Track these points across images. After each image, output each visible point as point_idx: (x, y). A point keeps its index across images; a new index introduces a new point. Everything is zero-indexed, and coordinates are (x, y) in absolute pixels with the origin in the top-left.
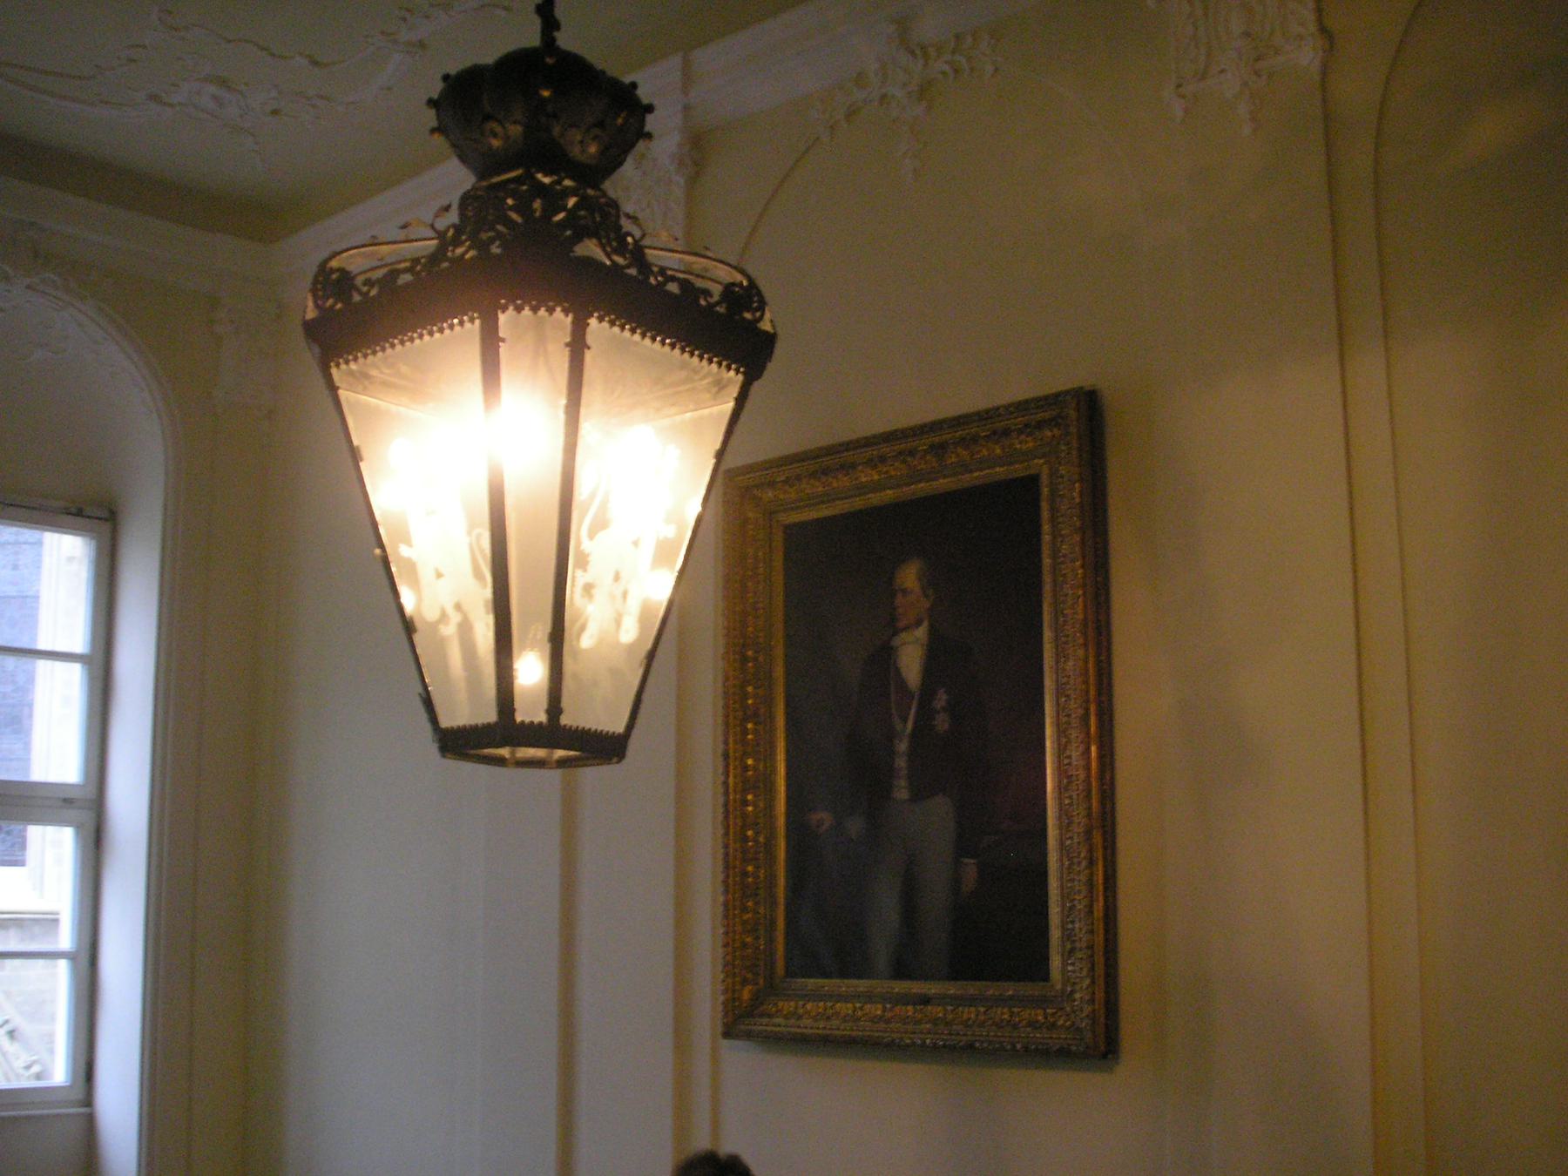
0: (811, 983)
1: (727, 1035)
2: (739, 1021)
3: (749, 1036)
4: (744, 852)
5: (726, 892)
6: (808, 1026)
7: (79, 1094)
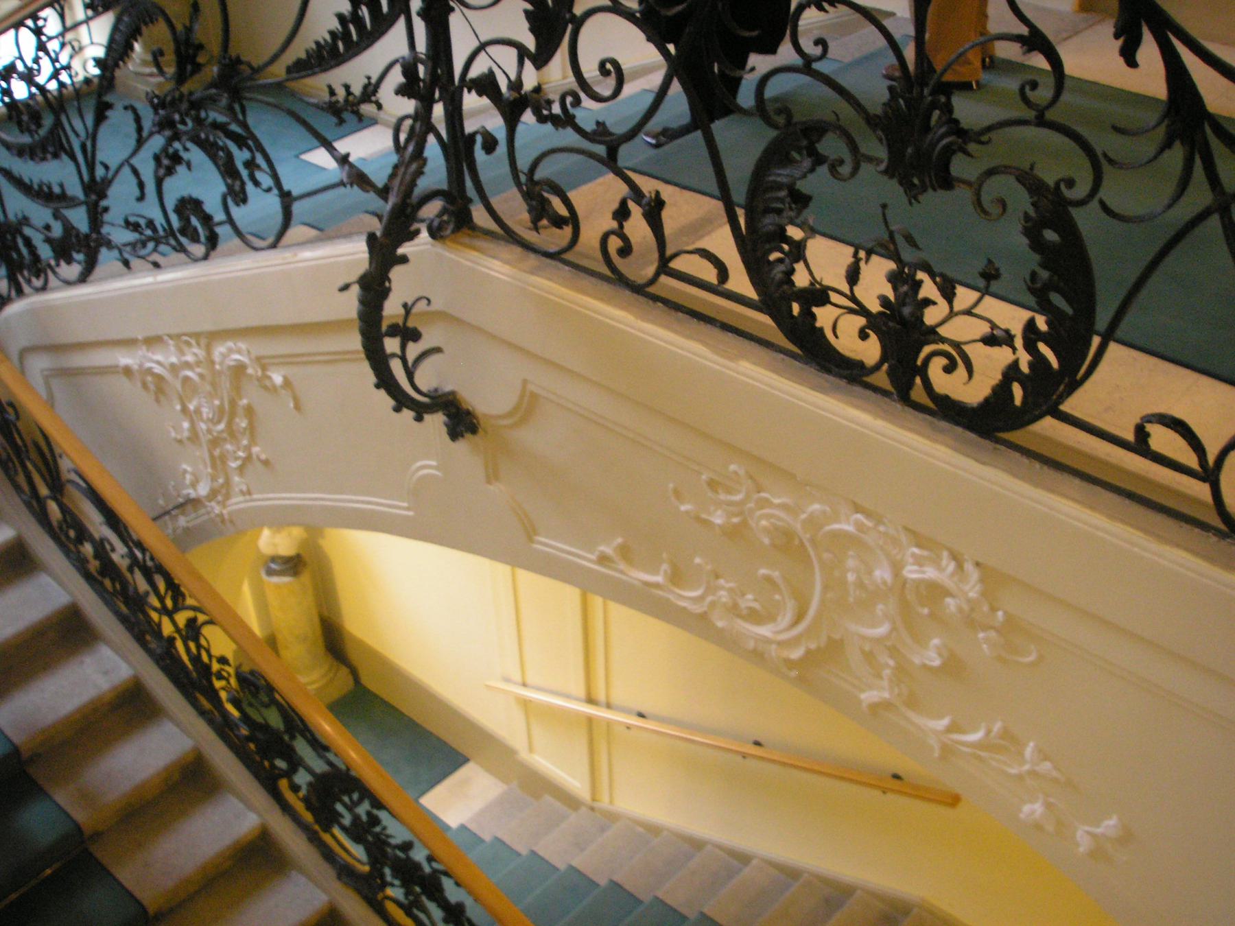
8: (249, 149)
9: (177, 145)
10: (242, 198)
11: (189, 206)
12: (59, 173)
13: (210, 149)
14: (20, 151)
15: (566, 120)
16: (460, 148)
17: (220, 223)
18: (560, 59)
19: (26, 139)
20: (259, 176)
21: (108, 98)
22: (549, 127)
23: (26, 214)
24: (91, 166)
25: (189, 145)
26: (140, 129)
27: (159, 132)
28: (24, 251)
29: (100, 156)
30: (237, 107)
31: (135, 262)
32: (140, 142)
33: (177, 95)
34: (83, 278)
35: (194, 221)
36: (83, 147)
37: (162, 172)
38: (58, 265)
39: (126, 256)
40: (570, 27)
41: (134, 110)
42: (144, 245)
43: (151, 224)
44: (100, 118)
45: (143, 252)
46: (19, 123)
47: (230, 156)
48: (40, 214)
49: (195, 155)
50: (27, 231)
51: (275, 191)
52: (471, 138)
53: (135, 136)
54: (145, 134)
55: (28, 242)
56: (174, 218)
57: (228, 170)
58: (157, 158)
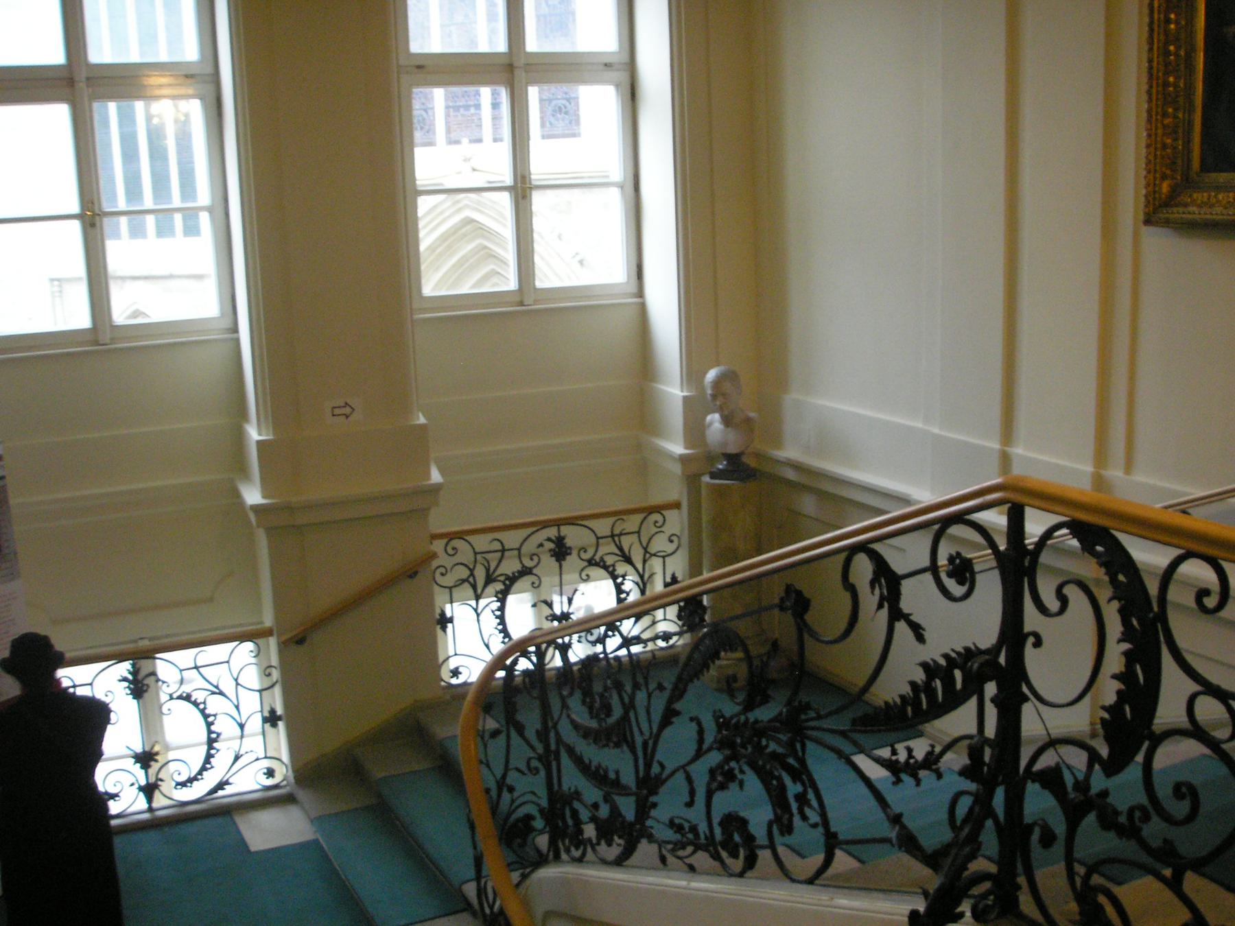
0: (1223, 177)
1: (1148, 222)
2: (1159, 211)
3: (1167, 223)
4: (1167, 64)
5: (1150, 100)
6: (1218, 214)
7: (633, 288)
8: (803, 784)
9: (733, 764)
10: (788, 829)
11: (734, 822)
12: (619, 762)
13: (765, 777)
14: (586, 733)
15: (1130, 831)
16: (1016, 835)
17: (762, 847)
18: (1133, 772)
19: (594, 724)
20: (808, 811)
21: (678, 706)
22: (1111, 835)
23: (580, 789)
24: (648, 766)
25: (746, 768)
26: (701, 741)
27: (719, 749)
28: (570, 822)
29: (658, 757)
30: (798, 746)
31: (670, 859)
32: (699, 754)
33: (743, 718)
34: (619, 862)
35: (737, 838)
36: (645, 744)
37: (714, 785)
38: (598, 844)
39: (664, 852)
40: (1146, 744)
41: (699, 724)
42: (684, 848)
43: (694, 829)
44: (666, 721)
45: (681, 853)
46: (591, 708)
47: (782, 788)
48: (591, 793)
49: (752, 782)
50: (576, 805)
51: (821, 829)
52: (1030, 828)
53: (694, 746)
54: (705, 747)
55: (575, 814)
56: (718, 831)
57: (778, 798)
58: (712, 772)
